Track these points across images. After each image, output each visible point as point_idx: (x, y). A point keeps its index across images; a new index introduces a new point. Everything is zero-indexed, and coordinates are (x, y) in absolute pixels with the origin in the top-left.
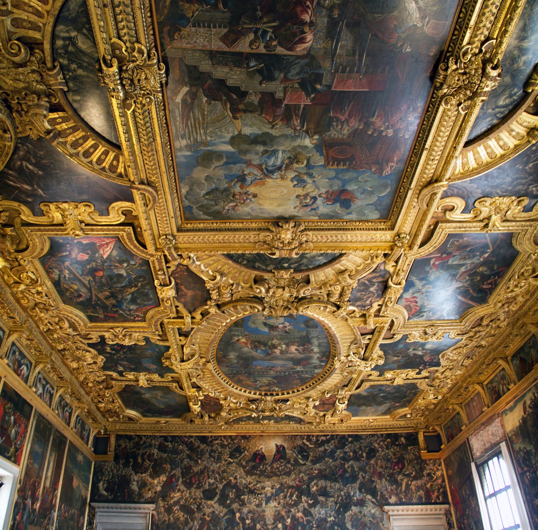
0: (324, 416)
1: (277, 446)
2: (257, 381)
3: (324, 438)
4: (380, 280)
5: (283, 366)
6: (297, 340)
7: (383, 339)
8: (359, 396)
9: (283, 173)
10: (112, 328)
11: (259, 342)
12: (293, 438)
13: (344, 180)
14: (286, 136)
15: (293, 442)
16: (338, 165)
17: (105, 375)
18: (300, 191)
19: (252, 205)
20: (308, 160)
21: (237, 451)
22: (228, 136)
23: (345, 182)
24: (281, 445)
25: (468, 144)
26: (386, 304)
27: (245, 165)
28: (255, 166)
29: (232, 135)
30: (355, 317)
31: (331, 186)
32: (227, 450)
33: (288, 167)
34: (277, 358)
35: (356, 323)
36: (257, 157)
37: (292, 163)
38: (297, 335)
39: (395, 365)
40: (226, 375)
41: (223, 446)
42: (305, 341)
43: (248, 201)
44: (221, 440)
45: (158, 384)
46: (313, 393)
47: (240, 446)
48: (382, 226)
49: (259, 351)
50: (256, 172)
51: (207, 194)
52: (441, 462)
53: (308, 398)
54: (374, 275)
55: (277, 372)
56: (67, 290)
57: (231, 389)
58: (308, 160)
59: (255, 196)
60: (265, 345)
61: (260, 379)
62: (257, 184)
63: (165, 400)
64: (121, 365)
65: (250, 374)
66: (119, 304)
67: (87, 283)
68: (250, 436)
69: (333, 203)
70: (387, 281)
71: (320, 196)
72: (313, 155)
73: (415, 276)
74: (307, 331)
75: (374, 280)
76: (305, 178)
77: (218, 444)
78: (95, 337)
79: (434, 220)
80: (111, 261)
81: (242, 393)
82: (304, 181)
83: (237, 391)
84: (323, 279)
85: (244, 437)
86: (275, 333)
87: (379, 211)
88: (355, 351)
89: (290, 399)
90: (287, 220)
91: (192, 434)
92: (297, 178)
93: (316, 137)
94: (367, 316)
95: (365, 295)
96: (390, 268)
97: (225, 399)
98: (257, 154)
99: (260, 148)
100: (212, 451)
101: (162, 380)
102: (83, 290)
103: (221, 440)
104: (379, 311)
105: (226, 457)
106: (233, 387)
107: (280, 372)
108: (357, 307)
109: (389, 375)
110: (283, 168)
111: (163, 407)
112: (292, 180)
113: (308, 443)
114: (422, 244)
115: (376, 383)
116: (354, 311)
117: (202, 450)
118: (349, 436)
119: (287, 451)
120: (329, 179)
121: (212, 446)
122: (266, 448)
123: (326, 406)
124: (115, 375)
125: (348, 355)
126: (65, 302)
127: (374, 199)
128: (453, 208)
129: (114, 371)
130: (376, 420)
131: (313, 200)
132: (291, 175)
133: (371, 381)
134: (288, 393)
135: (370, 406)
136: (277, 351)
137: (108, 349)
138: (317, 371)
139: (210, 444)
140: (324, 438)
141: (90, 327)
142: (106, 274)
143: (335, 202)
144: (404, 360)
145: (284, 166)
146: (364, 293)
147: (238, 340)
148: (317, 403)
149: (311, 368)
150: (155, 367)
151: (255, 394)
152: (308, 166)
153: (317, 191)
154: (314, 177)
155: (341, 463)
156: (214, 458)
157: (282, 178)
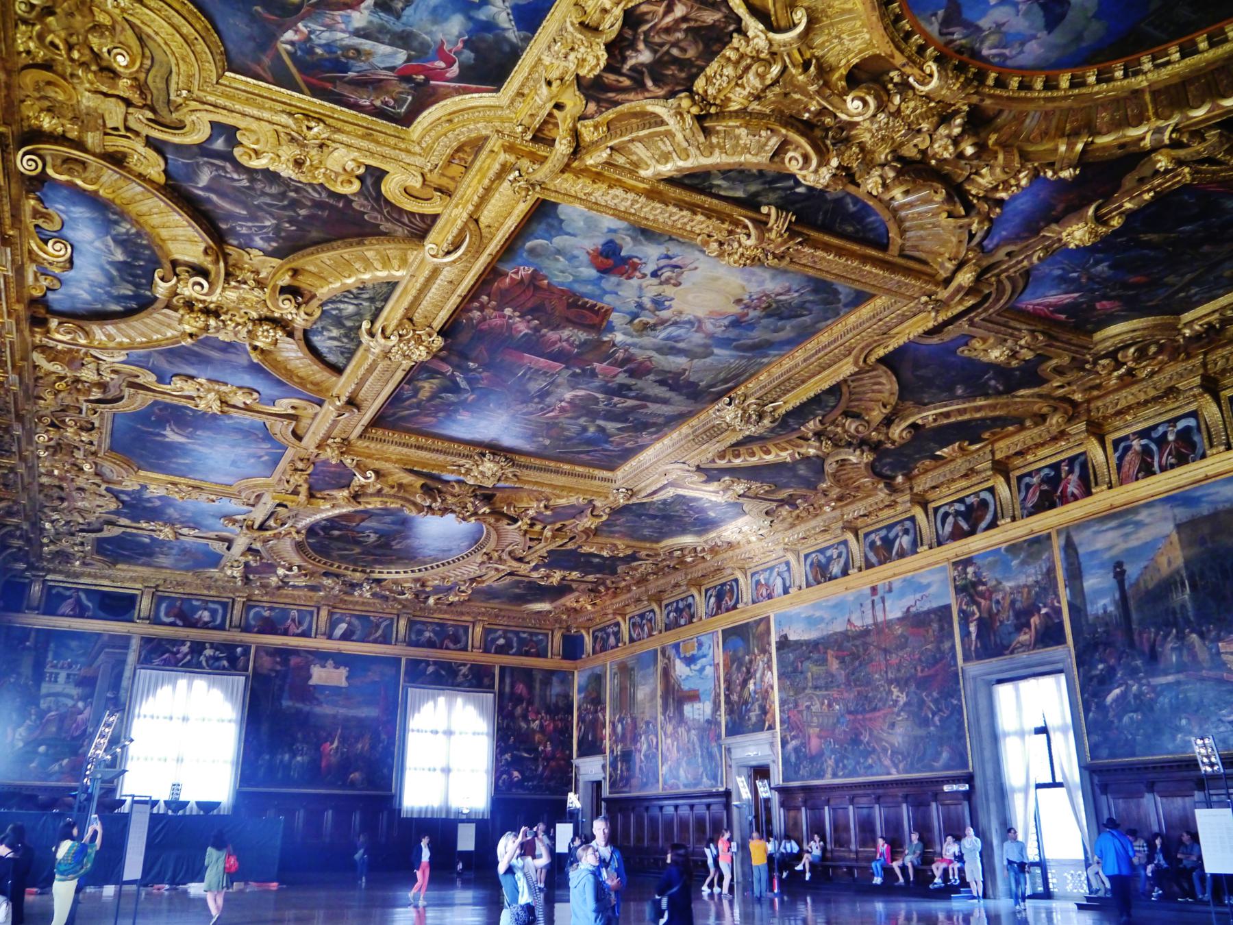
13: (595, 284)
18: (669, 290)
20: (631, 322)
22: (708, 360)
23: (596, 282)
31: (618, 284)
37: (655, 325)
59: (739, 301)
69: (630, 258)
71: (644, 276)
73: (507, 40)
75: (627, 82)
82: (654, 301)
95: (675, 44)
127: (559, 241)
132: (664, 314)
146: (675, 52)
153: (644, 285)
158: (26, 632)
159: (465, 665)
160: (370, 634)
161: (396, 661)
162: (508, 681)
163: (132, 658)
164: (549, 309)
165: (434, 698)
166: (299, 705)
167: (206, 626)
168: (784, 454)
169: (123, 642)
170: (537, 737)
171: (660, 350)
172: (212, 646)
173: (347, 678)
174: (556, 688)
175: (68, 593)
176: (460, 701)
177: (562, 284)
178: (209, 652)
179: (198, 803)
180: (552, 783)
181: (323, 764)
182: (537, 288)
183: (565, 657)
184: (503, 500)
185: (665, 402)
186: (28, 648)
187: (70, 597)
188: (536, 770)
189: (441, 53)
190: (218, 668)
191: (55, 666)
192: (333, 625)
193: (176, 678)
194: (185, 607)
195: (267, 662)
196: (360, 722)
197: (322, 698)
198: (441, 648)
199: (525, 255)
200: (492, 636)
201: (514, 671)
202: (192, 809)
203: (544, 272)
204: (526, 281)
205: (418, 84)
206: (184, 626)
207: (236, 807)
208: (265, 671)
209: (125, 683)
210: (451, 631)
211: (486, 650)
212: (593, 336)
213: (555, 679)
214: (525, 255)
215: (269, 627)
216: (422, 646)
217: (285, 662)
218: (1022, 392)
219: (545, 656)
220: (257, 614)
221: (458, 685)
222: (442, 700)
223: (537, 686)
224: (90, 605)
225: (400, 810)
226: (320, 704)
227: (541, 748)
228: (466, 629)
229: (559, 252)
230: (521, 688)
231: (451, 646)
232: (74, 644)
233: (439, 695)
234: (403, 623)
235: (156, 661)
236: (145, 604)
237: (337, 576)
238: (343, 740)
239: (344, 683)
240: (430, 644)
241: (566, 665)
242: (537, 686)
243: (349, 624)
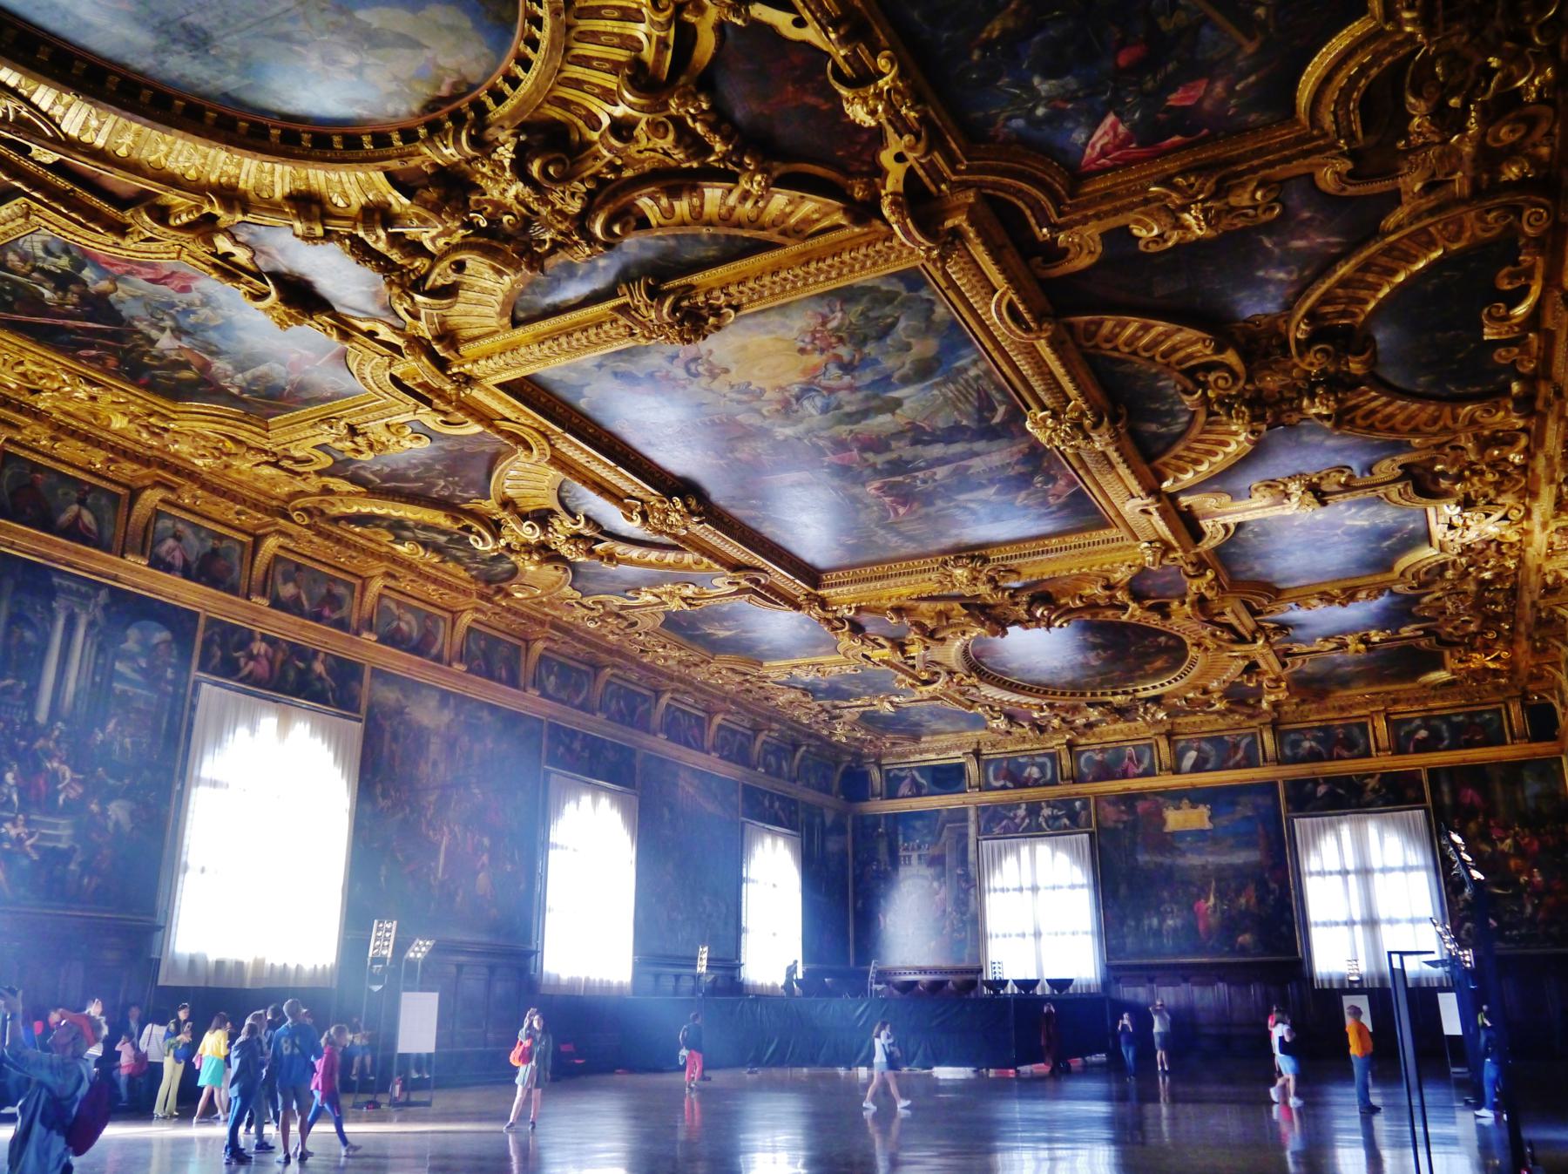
19: (795, 334)
22: (907, 404)
28: (840, 389)
50: (833, 383)
51: (893, 325)
98: (849, 403)
99: (848, 409)
112: (762, 391)
152: (759, 412)
157: (781, 389)
158: (876, 818)
159: (1372, 776)
160: (1230, 758)
161: (1269, 787)
162: (1445, 788)
163: (972, 830)
165: (1332, 826)
166: (1159, 859)
167: (1036, 783)
168: (1242, 438)
169: (960, 815)
170: (1512, 863)
172: (1049, 804)
173: (1210, 818)
174: (1532, 786)
175: (903, 774)
176: (1372, 828)
178: (1046, 812)
179: (1016, 982)
180: (1554, 930)
181: (1201, 927)
183: (1536, 738)
184: (1064, 593)
185: (977, 454)
186: (881, 835)
187: (904, 778)
188: (1522, 911)
190: (1059, 828)
191: (906, 849)
192: (1178, 756)
193: (1018, 846)
194: (1012, 767)
195: (1111, 814)
196: (1238, 871)
197: (1183, 846)
198: (1331, 759)
200: (1406, 728)
201: (1452, 771)
202: (1011, 989)
206: (1015, 788)
207: (1105, 984)
208: (1111, 824)
209: (971, 857)
210: (1340, 733)
211: (1399, 748)
213: (1526, 773)
215: (1106, 772)
216: (1303, 760)
217: (1131, 809)
218: (1390, 222)
219: (1504, 743)
220: (1089, 758)
221: (1369, 805)
222: (1345, 830)
223: (1498, 788)
224: (923, 781)
225: (1312, 979)
226: (1183, 853)
227: (1523, 879)
228: (1363, 728)
230: (1470, 795)
231: (1346, 754)
232: (918, 824)
233: (1340, 822)
234: (1268, 737)
235: (996, 830)
236: (972, 768)
237: (1102, 704)
238: (1221, 895)
239: (1208, 826)
240: (1313, 756)
241: (1541, 748)
242: (1498, 788)
243: (1199, 750)
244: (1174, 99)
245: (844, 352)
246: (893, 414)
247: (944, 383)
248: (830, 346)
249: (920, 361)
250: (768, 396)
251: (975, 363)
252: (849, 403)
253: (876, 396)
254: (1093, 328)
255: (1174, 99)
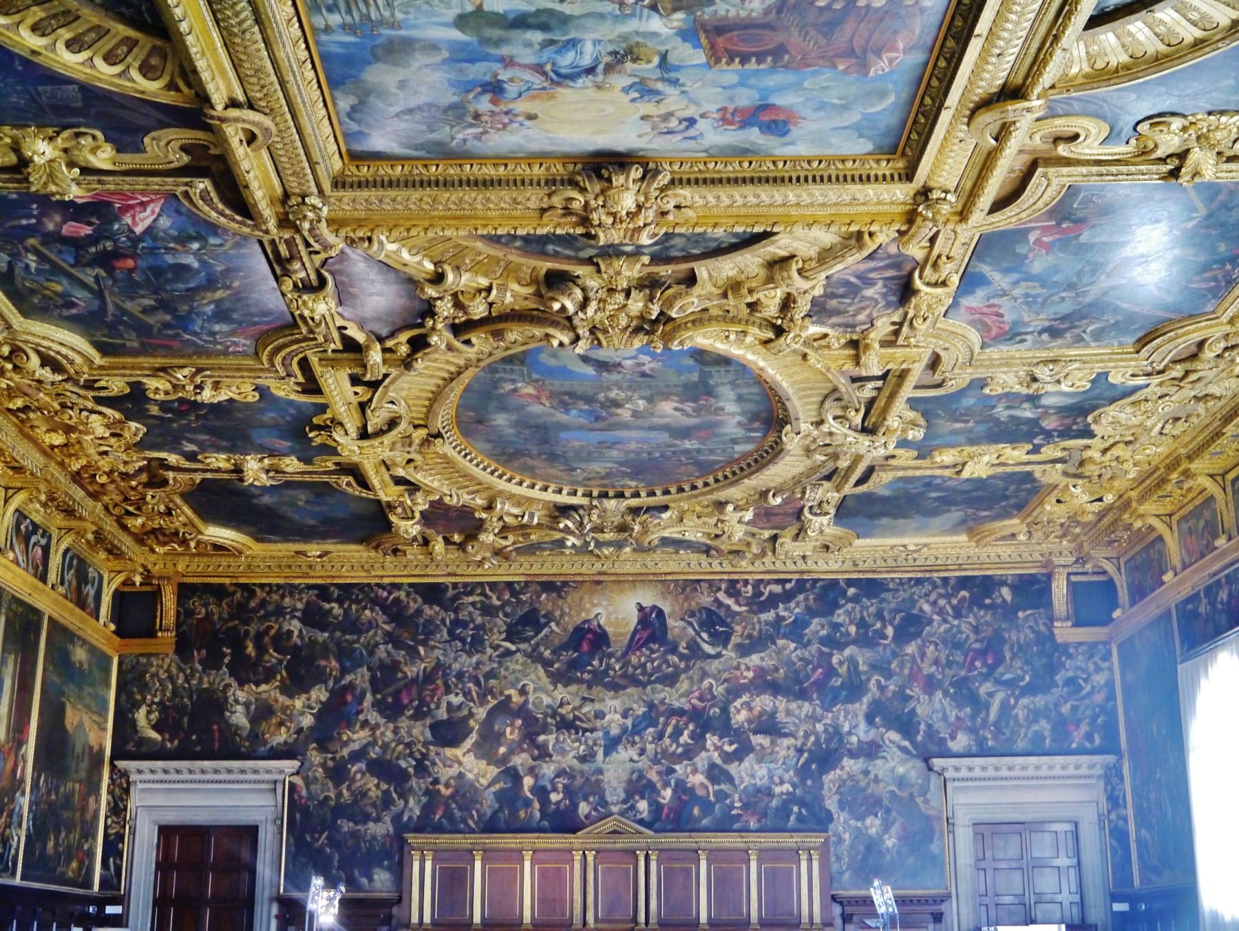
0: (774, 538)
1: (641, 608)
2: (574, 469)
3: (777, 589)
4: (891, 273)
5: (644, 441)
6: (675, 390)
7: (916, 387)
8: (869, 498)
9: (600, 78)
10: (163, 369)
11: (572, 394)
12: (689, 586)
13: (766, 89)
14: (602, 16)
15: (687, 599)
16: (744, 60)
17: (144, 459)
19: (524, 132)
20: (664, 57)
21: (527, 623)
24: (654, 607)
25: (1095, 21)
26: (911, 323)
27: (499, 65)
28: (525, 66)
29: (458, 11)
30: (828, 347)
32: (500, 621)
33: (609, 69)
34: (625, 426)
35: (833, 362)
36: (528, 51)
38: (674, 379)
39: (962, 439)
40: (489, 456)
41: (487, 610)
42: (699, 392)
43: (516, 125)
44: (483, 594)
45: (298, 478)
46: (734, 493)
47: (534, 611)
48: (884, 168)
49: (574, 412)
50: (528, 76)
52: (1109, 652)
53: (721, 505)
54: (872, 264)
55: (627, 452)
56: (33, 292)
57: (502, 485)
58: (664, 57)
59: (531, 117)
60: (589, 400)
61: (583, 466)
62: (533, 97)
63: (318, 509)
64: (191, 441)
65: (552, 457)
66: (183, 322)
67: (90, 281)
68: (565, 584)
70: (910, 275)
71: (703, 116)
72: (675, 48)
73: (989, 264)
74: (701, 371)
75: (872, 275)
76: (660, 86)
77: (473, 604)
78: (117, 385)
79: (1026, 159)
80: (155, 239)
81: (536, 493)
82: (658, 93)
83: (523, 491)
84: (731, 274)
85: (549, 586)
86: (615, 377)
87: (869, 138)
88: (839, 412)
89: (672, 505)
90: (620, 160)
91: (398, 580)
92: (638, 87)
93: (680, 15)
94: (861, 346)
95: (850, 305)
96: (916, 250)
97: (489, 508)
98: (528, 45)
99: (537, 37)
100: (457, 623)
101: (310, 468)
102: (79, 295)
103: (483, 594)
104: (896, 333)
105: (497, 638)
106: (509, 480)
107: (637, 453)
108: (833, 326)
109: (947, 457)
110: (601, 68)
111: (312, 522)
112: (626, 90)
113: (730, 602)
114: (1000, 205)
115: (910, 473)
116: (825, 336)
117: (430, 621)
118: (850, 583)
119: (670, 622)
120: (724, 88)
121: (456, 611)
122: (609, 614)
123: (777, 519)
124: (173, 459)
125: (819, 423)
126: (25, 314)
127: (854, 117)
128: (1076, 137)
129: (172, 450)
130: (925, 545)
131: (685, 124)
132: (619, 81)
133: (896, 468)
134: (666, 492)
135: (904, 517)
136: (625, 414)
137: (154, 410)
138: (738, 448)
139: (451, 605)
140: (777, 589)
141: (101, 367)
142: (142, 263)
143: (744, 125)
144: (981, 429)
145: (601, 68)
146: (847, 301)
147: (515, 390)
148: (749, 515)
149: (724, 443)
150: (289, 444)
151: (575, 493)
154: (683, 85)
155: (821, 653)
156: (463, 640)
157: (599, 87)
164: (813, 33)
171: (565, 20)
177: (814, 73)
182: (850, 53)
189: (1048, 247)
199: (890, 86)
203: (852, 78)
204: (871, 57)
205: (1066, 219)
212: (706, 13)
214: (890, 86)
229: (844, 108)
244: (87, 230)
245: (484, 104)
246: (479, 8)
247: (382, 22)
248: (493, 113)
249: (396, 64)
250: (628, 81)
251: (328, 30)
252: (528, 45)
253: (485, 41)
254: (154, 61)
255: (87, 230)
